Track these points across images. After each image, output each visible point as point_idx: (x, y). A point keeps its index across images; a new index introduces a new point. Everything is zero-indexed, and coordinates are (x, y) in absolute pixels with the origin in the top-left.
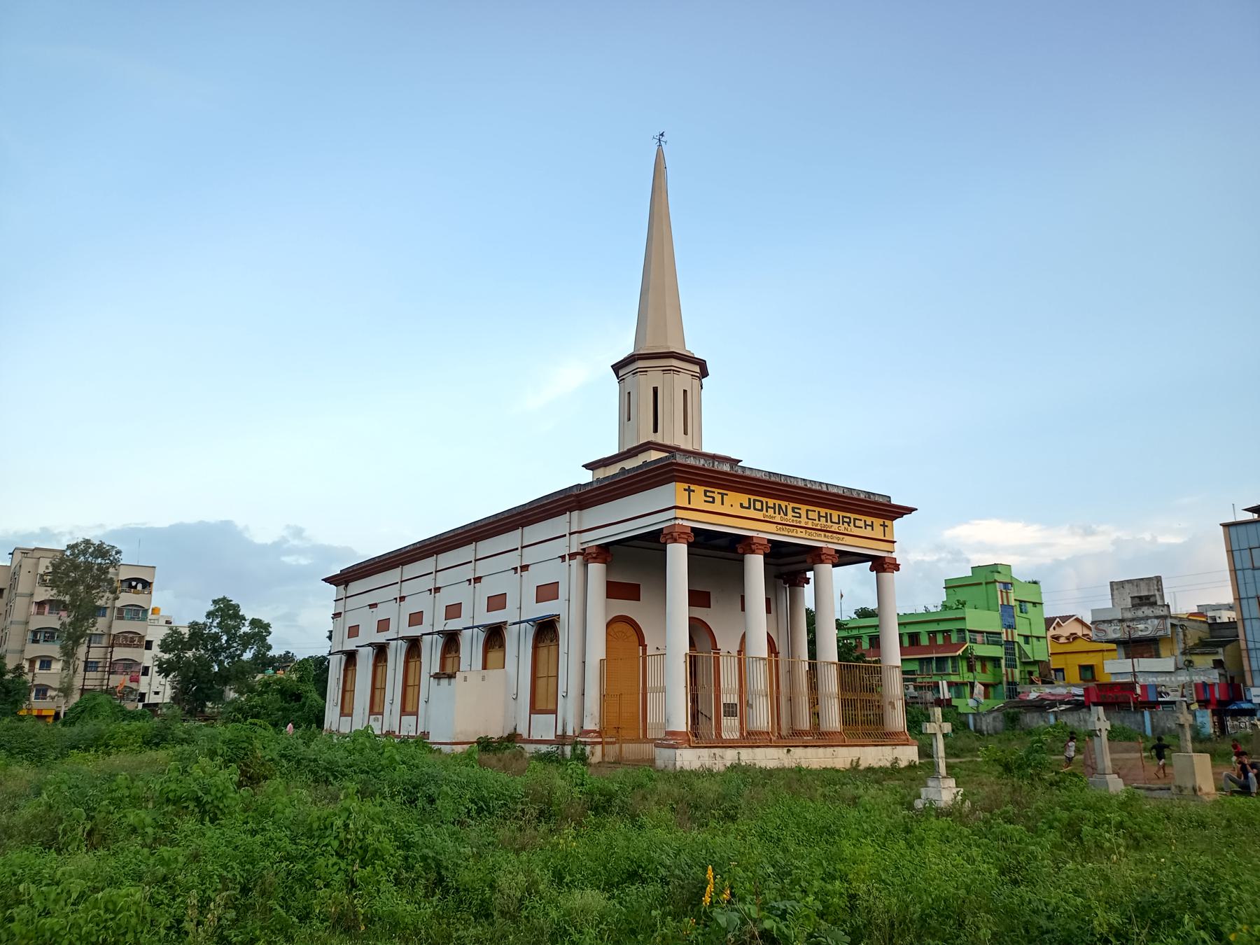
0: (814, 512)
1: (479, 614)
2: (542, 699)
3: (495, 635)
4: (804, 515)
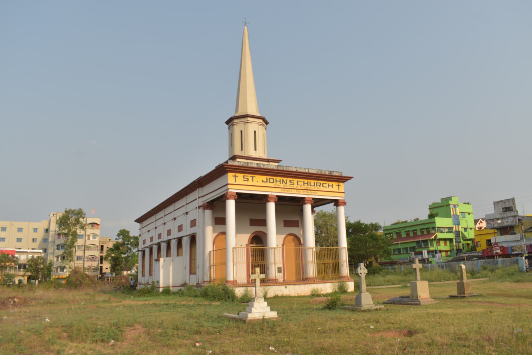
0: (301, 181)
4: (295, 183)
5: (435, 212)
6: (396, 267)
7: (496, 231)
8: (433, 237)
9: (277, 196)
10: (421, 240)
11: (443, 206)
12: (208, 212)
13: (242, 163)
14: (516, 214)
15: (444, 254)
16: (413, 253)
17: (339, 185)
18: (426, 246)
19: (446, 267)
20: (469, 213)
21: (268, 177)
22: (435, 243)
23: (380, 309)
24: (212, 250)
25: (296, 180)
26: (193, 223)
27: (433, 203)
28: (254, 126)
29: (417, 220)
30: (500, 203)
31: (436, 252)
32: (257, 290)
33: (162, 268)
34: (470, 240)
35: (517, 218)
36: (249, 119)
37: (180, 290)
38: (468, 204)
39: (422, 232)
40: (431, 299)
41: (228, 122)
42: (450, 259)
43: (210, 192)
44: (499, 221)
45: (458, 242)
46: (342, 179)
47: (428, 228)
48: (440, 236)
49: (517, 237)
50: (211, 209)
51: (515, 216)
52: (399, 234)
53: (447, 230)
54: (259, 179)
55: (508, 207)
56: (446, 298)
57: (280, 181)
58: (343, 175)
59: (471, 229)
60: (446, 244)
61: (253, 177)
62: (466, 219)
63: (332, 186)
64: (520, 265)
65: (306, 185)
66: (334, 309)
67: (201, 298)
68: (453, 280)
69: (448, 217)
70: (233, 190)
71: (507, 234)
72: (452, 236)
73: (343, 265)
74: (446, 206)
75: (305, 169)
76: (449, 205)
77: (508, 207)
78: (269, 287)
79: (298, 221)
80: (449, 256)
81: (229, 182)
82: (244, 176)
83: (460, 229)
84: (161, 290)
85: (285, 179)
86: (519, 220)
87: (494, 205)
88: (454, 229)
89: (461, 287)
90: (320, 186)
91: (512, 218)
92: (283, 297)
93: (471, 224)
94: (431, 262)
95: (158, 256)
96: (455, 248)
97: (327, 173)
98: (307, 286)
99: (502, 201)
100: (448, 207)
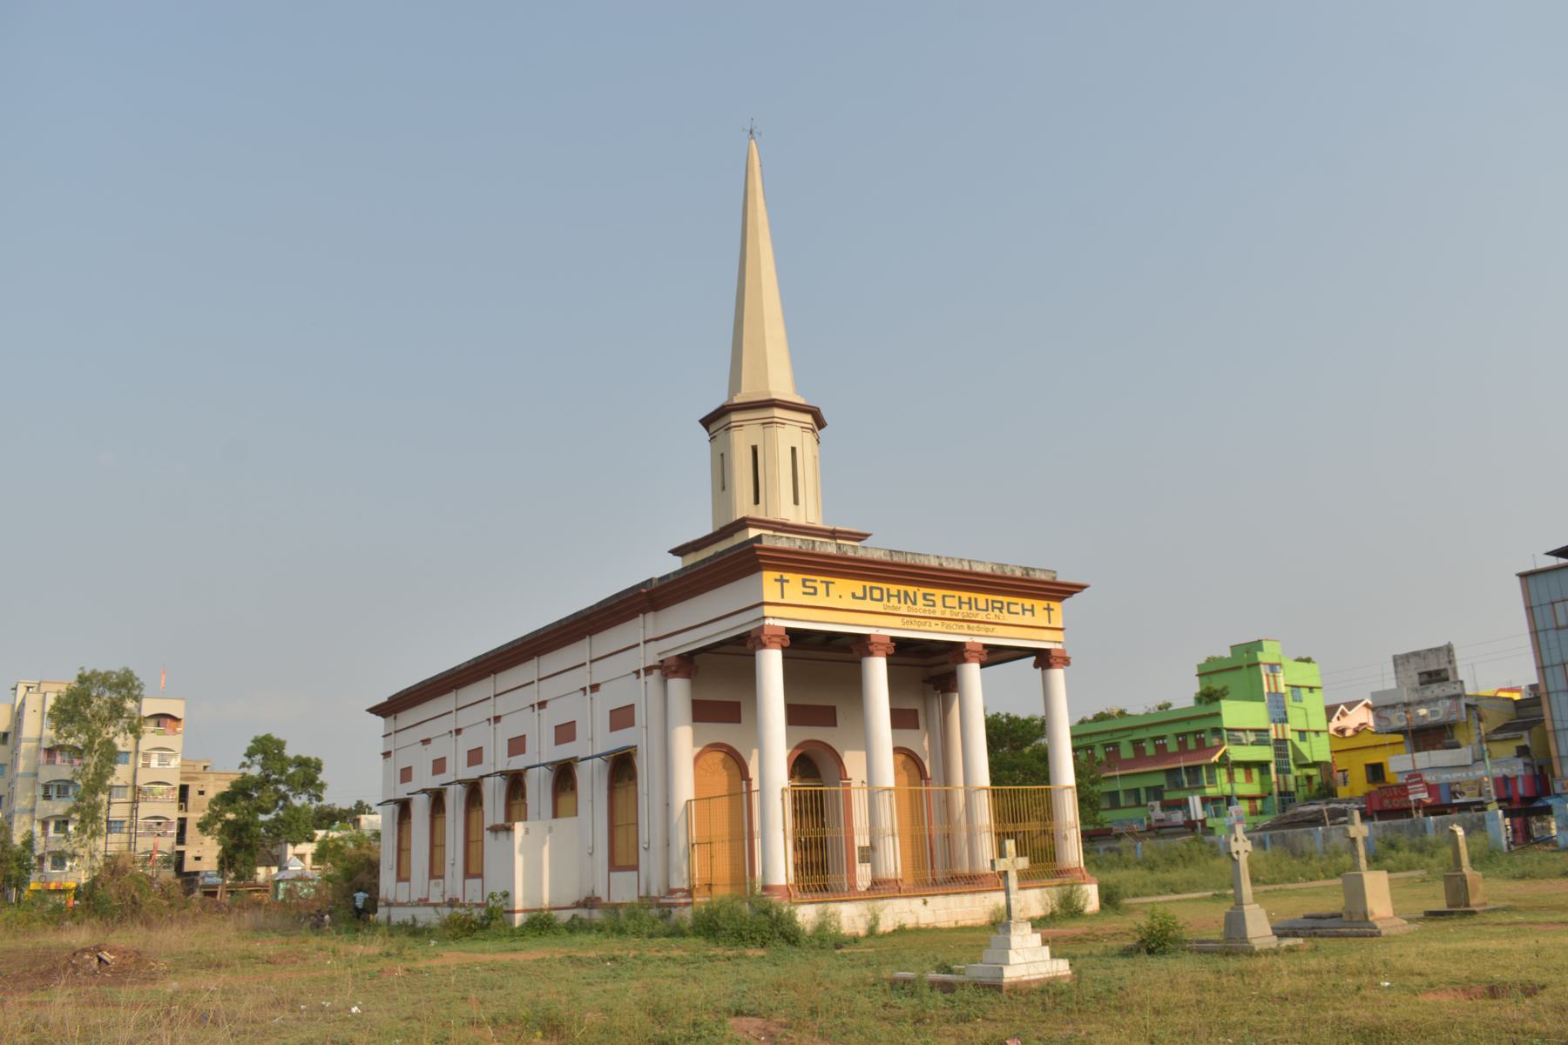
1: (544, 751)
2: (621, 857)
3: (564, 775)
5: (1217, 683)
6: (1123, 844)
7: (1400, 738)
8: (1215, 758)
9: (893, 639)
10: (1182, 765)
11: (1239, 668)
12: (679, 688)
13: (798, 543)
14: (1458, 691)
15: (1244, 806)
16: (1157, 804)
17: (1049, 609)
18: (1196, 785)
19: (1273, 842)
20: (1311, 689)
21: (869, 584)
22: (1222, 775)
23: (1290, 950)
24: (691, 796)
25: (939, 593)
26: (622, 718)
27: (1209, 660)
28: (791, 433)
29: (1165, 707)
30: (1412, 660)
31: (1229, 800)
32: (1013, 902)
33: (521, 852)
34: (1315, 764)
35: (1463, 701)
36: (778, 412)
37: (574, 916)
38: (1308, 660)
39: (1183, 744)
40: (1398, 921)
41: (707, 422)
42: (1265, 820)
43: (701, 621)
44: (1423, 711)
45: (1283, 770)
46: (1057, 591)
47: (1201, 732)
48: (1238, 753)
49: (1463, 755)
50: (688, 675)
51: (1457, 697)
52: (1113, 750)
53: (1252, 737)
54: (844, 590)
55: (1434, 671)
56: (1418, 919)
57: (898, 596)
58: (1061, 578)
59: (1317, 732)
60: (1249, 779)
61: (827, 583)
62: (1303, 705)
63: (1032, 610)
64: (1490, 834)
65: (965, 607)
66: (1163, 953)
67: (692, 940)
68: (1327, 877)
69: (1252, 699)
70: (779, 620)
71: (1434, 749)
72: (1265, 753)
73: (1066, 838)
74: (1249, 666)
75: (961, 560)
76: (1258, 664)
77: (1434, 671)
78: (880, 903)
79: (916, 711)
80: (1261, 813)
81: (766, 599)
82: (804, 581)
83: (1289, 735)
84: (519, 919)
85: (911, 590)
86: (1467, 706)
87: (1396, 666)
88: (1273, 735)
89: (1458, 891)
90: (1000, 609)
91: (1448, 703)
92: (918, 930)
93: (1318, 721)
94: (1211, 831)
95: (509, 817)
96: (1275, 788)
97: (1018, 573)
98: (978, 897)
99: (1416, 654)
100: (1253, 669)
